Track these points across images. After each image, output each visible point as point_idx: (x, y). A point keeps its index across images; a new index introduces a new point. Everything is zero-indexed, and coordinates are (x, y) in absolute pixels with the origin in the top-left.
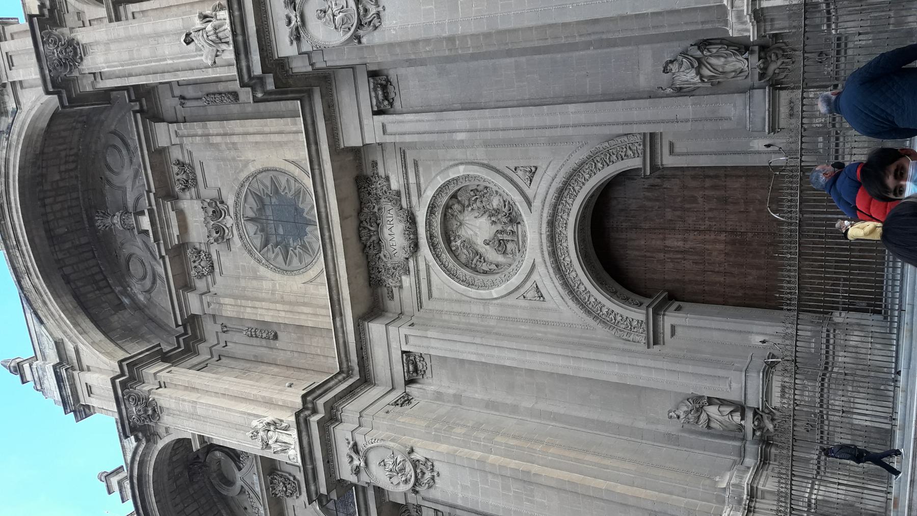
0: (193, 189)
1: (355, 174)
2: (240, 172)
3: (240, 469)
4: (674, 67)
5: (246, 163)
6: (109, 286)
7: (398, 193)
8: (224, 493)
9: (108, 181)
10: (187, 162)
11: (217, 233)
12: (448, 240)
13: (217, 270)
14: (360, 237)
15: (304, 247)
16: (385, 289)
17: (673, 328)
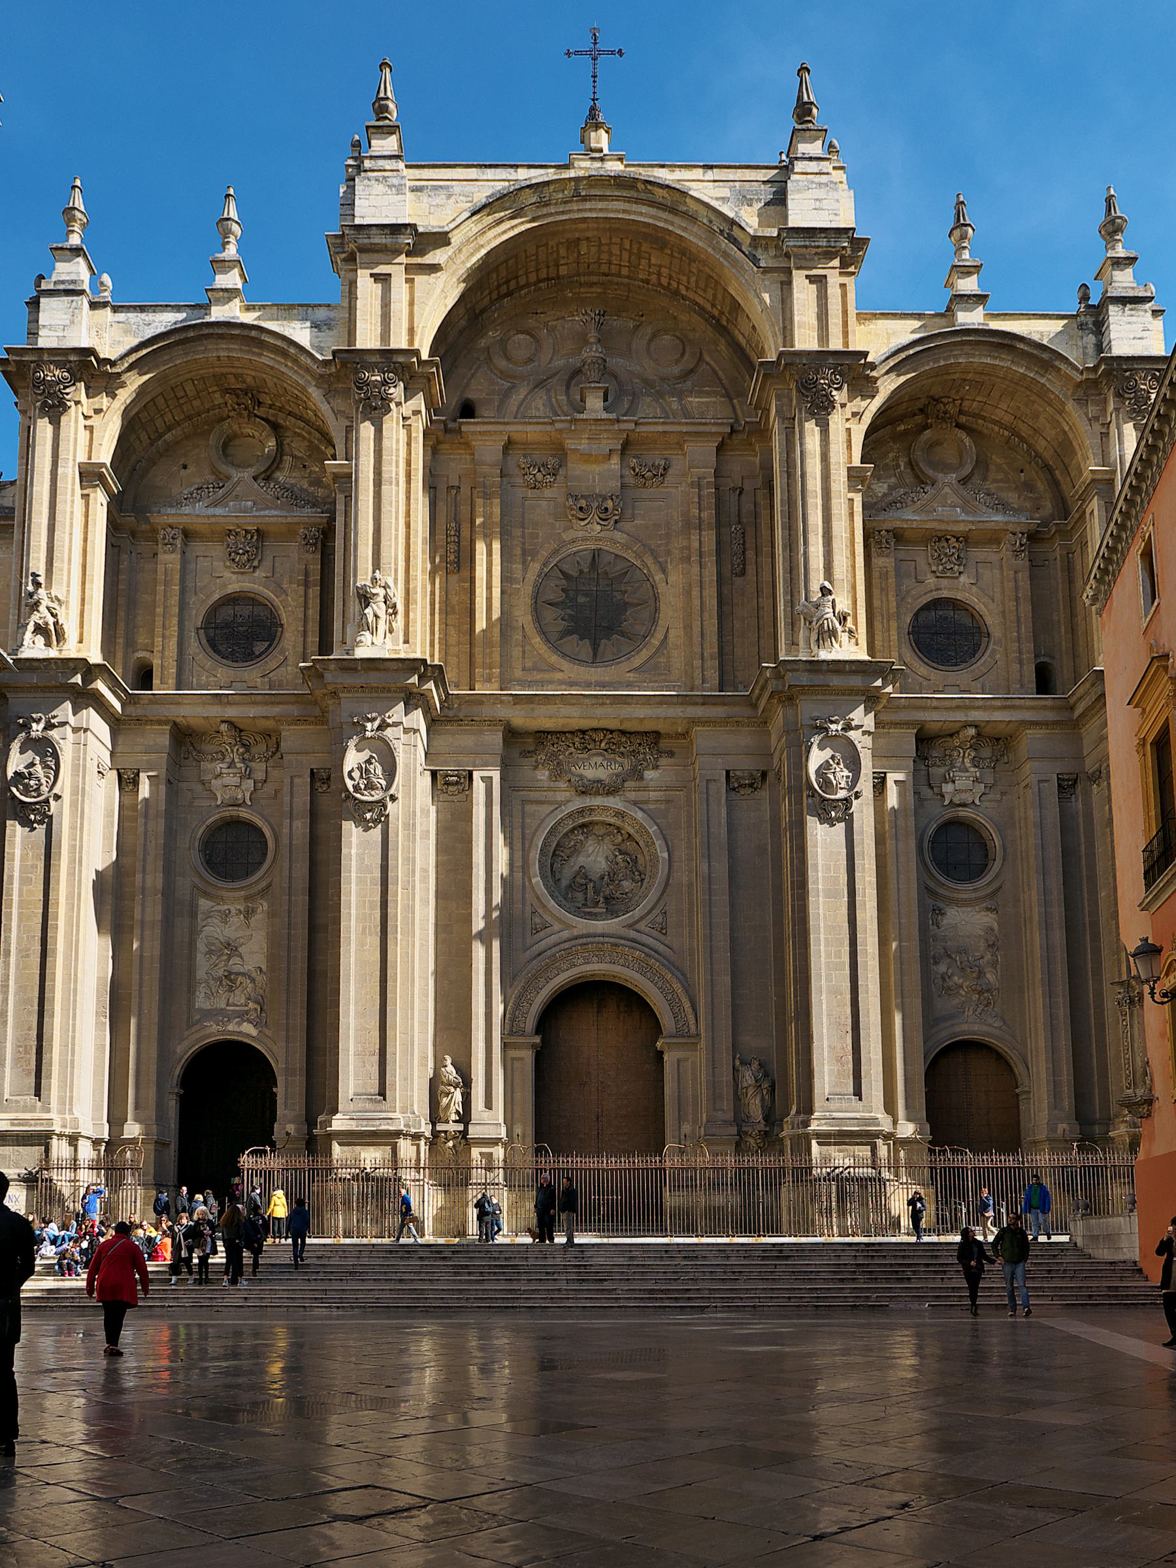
0: (631, 481)
1: (662, 731)
2: (655, 558)
3: (255, 478)
4: (755, 1065)
5: (664, 571)
6: (501, 297)
7: (642, 778)
8: (212, 440)
9: (637, 327)
10: (669, 478)
11: (581, 509)
12: (583, 826)
13: (530, 493)
14: (595, 730)
15: (566, 633)
16: (532, 748)
17: (522, 1059)
